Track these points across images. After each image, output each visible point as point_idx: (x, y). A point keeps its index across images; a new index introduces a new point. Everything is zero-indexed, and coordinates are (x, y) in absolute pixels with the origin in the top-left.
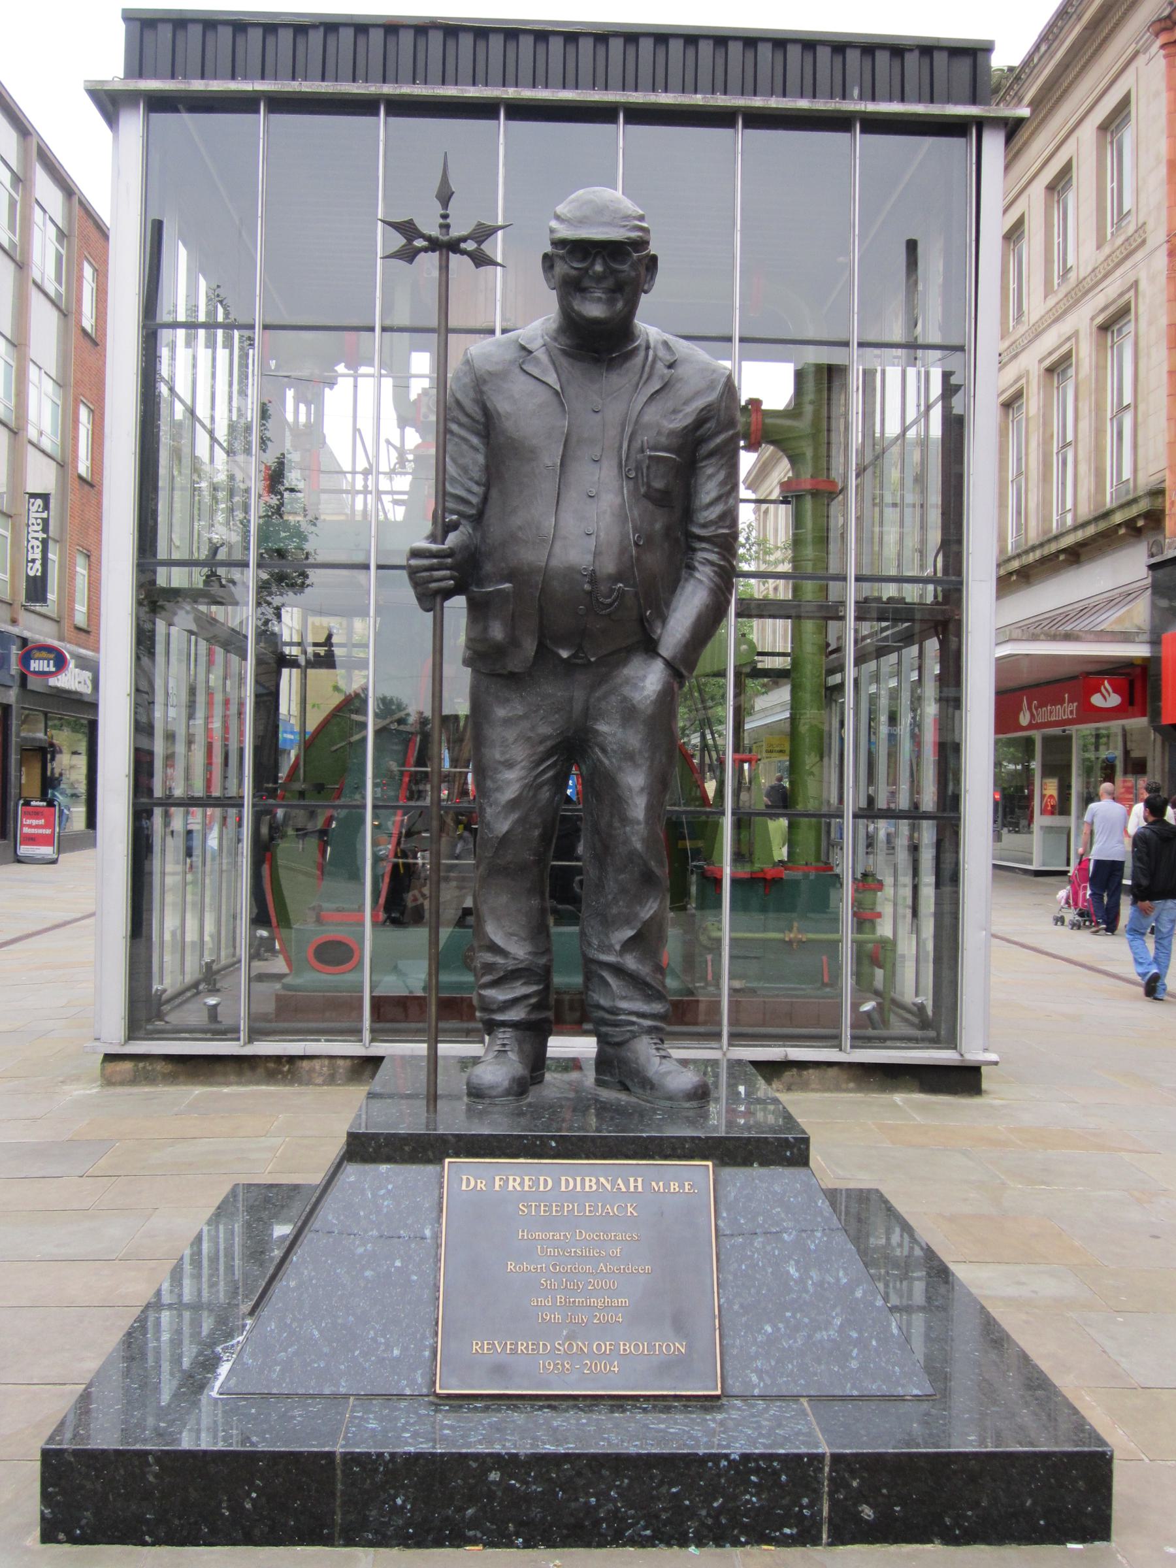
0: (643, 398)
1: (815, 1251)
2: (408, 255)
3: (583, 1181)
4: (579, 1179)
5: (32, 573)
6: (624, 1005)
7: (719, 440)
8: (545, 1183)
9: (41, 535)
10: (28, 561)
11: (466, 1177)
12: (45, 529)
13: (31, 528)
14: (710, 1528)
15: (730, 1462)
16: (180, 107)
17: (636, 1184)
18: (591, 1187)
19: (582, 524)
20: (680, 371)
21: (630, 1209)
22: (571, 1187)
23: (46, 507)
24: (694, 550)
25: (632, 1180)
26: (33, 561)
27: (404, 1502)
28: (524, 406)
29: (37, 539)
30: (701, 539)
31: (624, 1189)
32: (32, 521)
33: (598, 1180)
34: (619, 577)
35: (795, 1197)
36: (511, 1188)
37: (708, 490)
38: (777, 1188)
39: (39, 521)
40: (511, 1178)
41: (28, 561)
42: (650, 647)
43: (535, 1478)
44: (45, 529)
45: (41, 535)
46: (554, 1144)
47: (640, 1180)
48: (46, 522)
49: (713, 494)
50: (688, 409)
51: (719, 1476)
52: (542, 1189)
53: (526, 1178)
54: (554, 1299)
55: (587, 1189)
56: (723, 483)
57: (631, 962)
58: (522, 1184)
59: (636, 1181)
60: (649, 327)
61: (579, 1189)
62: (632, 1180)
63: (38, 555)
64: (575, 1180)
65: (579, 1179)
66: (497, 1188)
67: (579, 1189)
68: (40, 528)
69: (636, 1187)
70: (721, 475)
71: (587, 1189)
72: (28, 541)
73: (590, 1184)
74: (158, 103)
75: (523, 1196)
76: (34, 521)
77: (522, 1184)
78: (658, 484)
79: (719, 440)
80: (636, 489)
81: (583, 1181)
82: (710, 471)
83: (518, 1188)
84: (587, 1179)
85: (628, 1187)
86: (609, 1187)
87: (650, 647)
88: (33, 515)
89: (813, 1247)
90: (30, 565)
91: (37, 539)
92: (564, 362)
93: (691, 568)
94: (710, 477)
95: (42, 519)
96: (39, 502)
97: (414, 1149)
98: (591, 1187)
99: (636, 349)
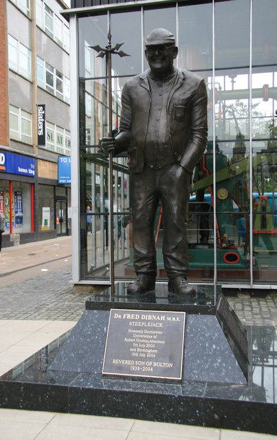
0: (173, 91)
2: (118, 46)
6: (173, 267)
14: (170, 417)
19: (159, 126)
20: (187, 81)
28: (141, 92)
30: (195, 130)
34: (166, 143)
78: (178, 115)
80: (172, 117)
92: (152, 81)
99: (172, 77)
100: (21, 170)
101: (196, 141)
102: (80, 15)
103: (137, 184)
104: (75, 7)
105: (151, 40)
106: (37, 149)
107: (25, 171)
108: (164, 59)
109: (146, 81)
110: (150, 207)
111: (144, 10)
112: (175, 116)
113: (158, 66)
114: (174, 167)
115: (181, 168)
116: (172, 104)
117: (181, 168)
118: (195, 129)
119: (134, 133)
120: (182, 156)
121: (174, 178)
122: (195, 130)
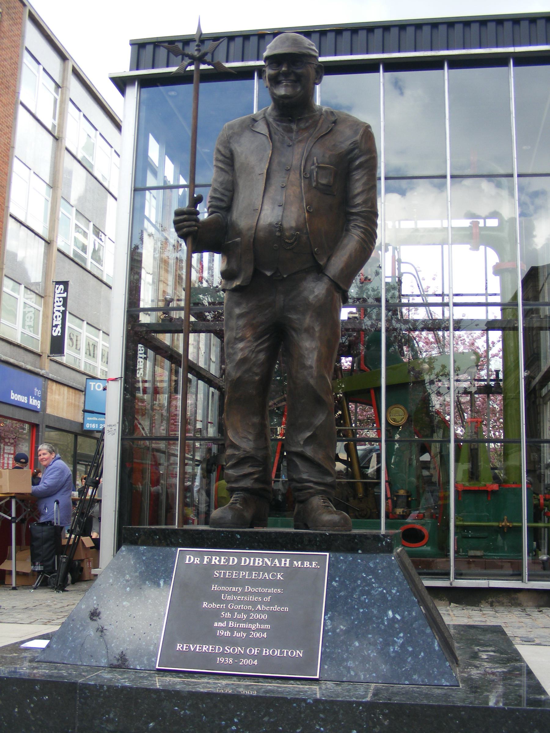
1: (391, 600)
3: (254, 560)
4: (252, 559)
5: (55, 334)
8: (233, 561)
9: (62, 309)
10: (53, 327)
12: (65, 305)
13: (56, 304)
15: (307, 704)
16: (158, 84)
17: (286, 562)
18: (259, 563)
21: (279, 576)
22: (247, 563)
23: (66, 290)
25: (283, 560)
26: (56, 326)
27: (114, 716)
29: (59, 311)
31: (278, 565)
32: (57, 299)
33: (263, 560)
35: (382, 570)
36: (213, 563)
38: (371, 565)
39: (61, 299)
40: (214, 558)
41: (53, 327)
43: (190, 706)
44: (65, 305)
45: (62, 309)
46: (239, 537)
47: (288, 560)
48: (65, 299)
51: (300, 712)
52: (231, 564)
53: (223, 558)
54: (228, 624)
55: (256, 564)
57: (309, 451)
58: (220, 561)
59: (285, 561)
61: (251, 564)
62: (283, 560)
63: (59, 322)
64: (250, 560)
65: (252, 559)
66: (205, 563)
67: (251, 564)
68: (61, 303)
69: (285, 564)
71: (256, 564)
72: (54, 313)
73: (259, 562)
74: (145, 82)
76: (58, 299)
77: (220, 561)
81: (254, 560)
83: (218, 563)
84: (257, 559)
85: (280, 564)
86: (269, 563)
88: (57, 295)
89: (389, 598)
90: (54, 328)
91: (59, 311)
94: (358, 180)
95: (63, 298)
96: (62, 287)
98: (259, 563)
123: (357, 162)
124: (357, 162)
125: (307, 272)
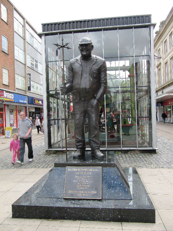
7: (103, 69)
11: (69, 169)
24: (101, 84)
30: (102, 83)
34: (89, 88)
37: (103, 76)
42: (95, 98)
49: (103, 77)
50: (99, 66)
56: (104, 75)
60: (93, 56)
70: (104, 74)
75: (76, 172)
79: (103, 69)
82: (102, 74)
87: (95, 98)
93: (101, 87)
97: (63, 166)
100: (20, 101)
101: (102, 88)
102: (46, 35)
103: (76, 107)
104: (44, 32)
105: (82, 42)
106: (27, 92)
107: (22, 101)
108: (87, 50)
109: (79, 60)
110: (82, 118)
111: (74, 33)
112: (93, 76)
113: (84, 53)
114: (93, 100)
115: (96, 100)
116: (91, 71)
117: (96, 100)
118: (102, 82)
119: (74, 84)
120: (97, 95)
121: (93, 105)
122: (102, 83)
123: (102, 70)
124: (102, 70)
125: (92, 98)
